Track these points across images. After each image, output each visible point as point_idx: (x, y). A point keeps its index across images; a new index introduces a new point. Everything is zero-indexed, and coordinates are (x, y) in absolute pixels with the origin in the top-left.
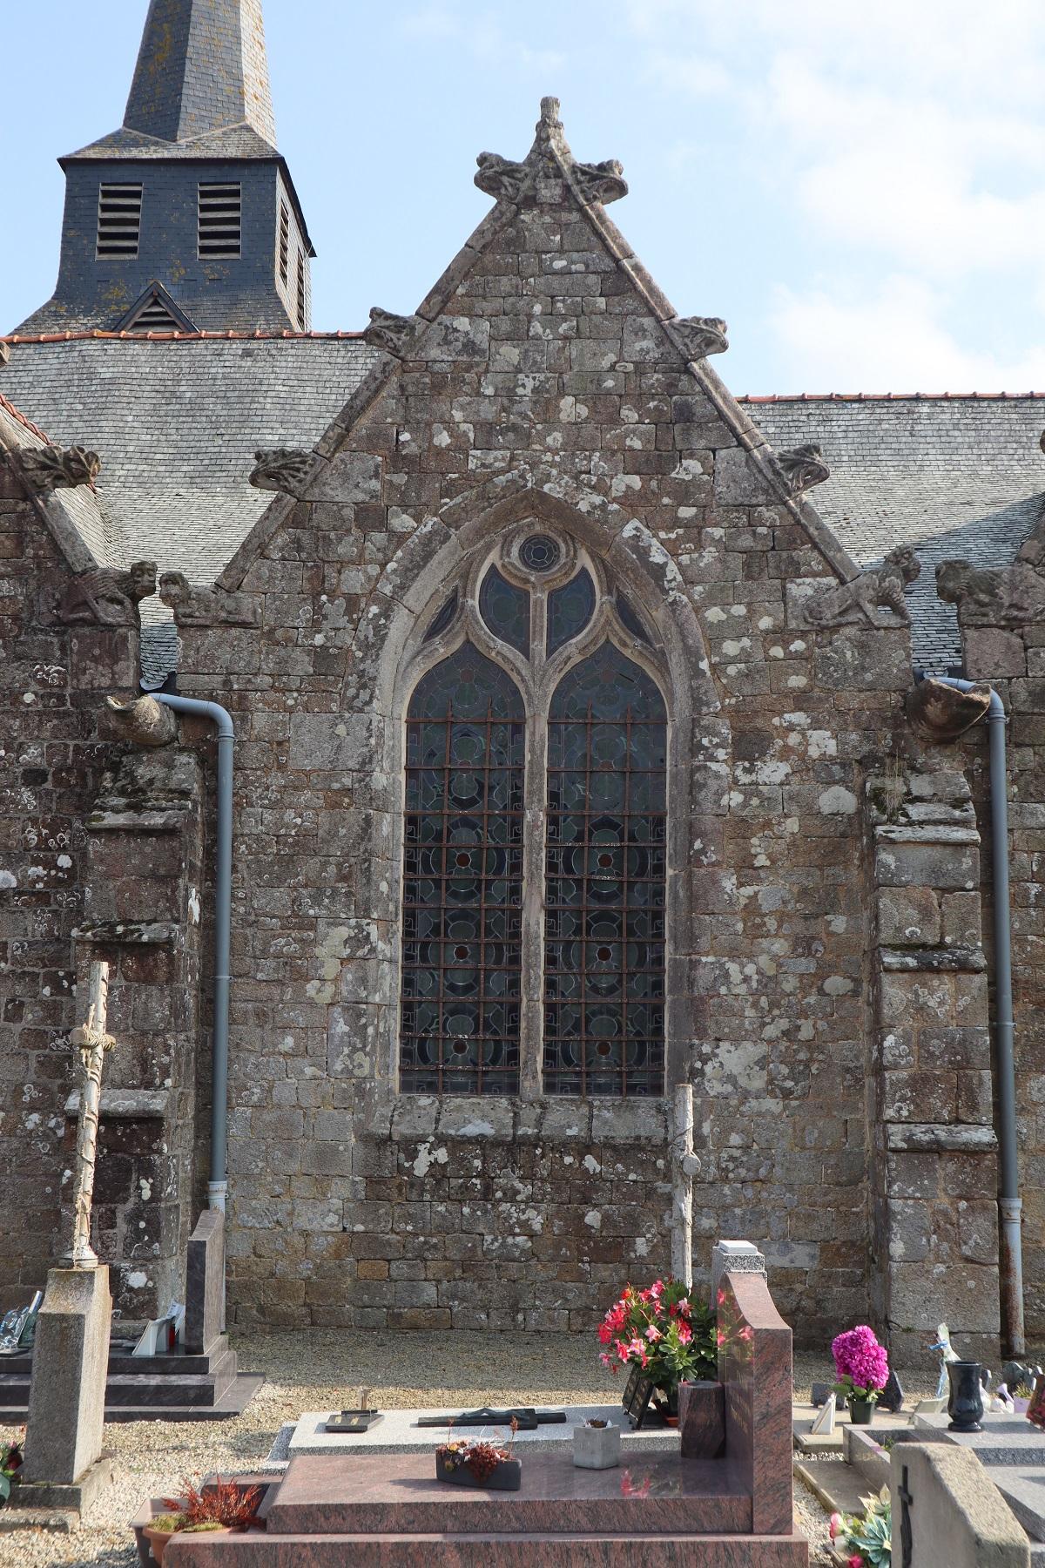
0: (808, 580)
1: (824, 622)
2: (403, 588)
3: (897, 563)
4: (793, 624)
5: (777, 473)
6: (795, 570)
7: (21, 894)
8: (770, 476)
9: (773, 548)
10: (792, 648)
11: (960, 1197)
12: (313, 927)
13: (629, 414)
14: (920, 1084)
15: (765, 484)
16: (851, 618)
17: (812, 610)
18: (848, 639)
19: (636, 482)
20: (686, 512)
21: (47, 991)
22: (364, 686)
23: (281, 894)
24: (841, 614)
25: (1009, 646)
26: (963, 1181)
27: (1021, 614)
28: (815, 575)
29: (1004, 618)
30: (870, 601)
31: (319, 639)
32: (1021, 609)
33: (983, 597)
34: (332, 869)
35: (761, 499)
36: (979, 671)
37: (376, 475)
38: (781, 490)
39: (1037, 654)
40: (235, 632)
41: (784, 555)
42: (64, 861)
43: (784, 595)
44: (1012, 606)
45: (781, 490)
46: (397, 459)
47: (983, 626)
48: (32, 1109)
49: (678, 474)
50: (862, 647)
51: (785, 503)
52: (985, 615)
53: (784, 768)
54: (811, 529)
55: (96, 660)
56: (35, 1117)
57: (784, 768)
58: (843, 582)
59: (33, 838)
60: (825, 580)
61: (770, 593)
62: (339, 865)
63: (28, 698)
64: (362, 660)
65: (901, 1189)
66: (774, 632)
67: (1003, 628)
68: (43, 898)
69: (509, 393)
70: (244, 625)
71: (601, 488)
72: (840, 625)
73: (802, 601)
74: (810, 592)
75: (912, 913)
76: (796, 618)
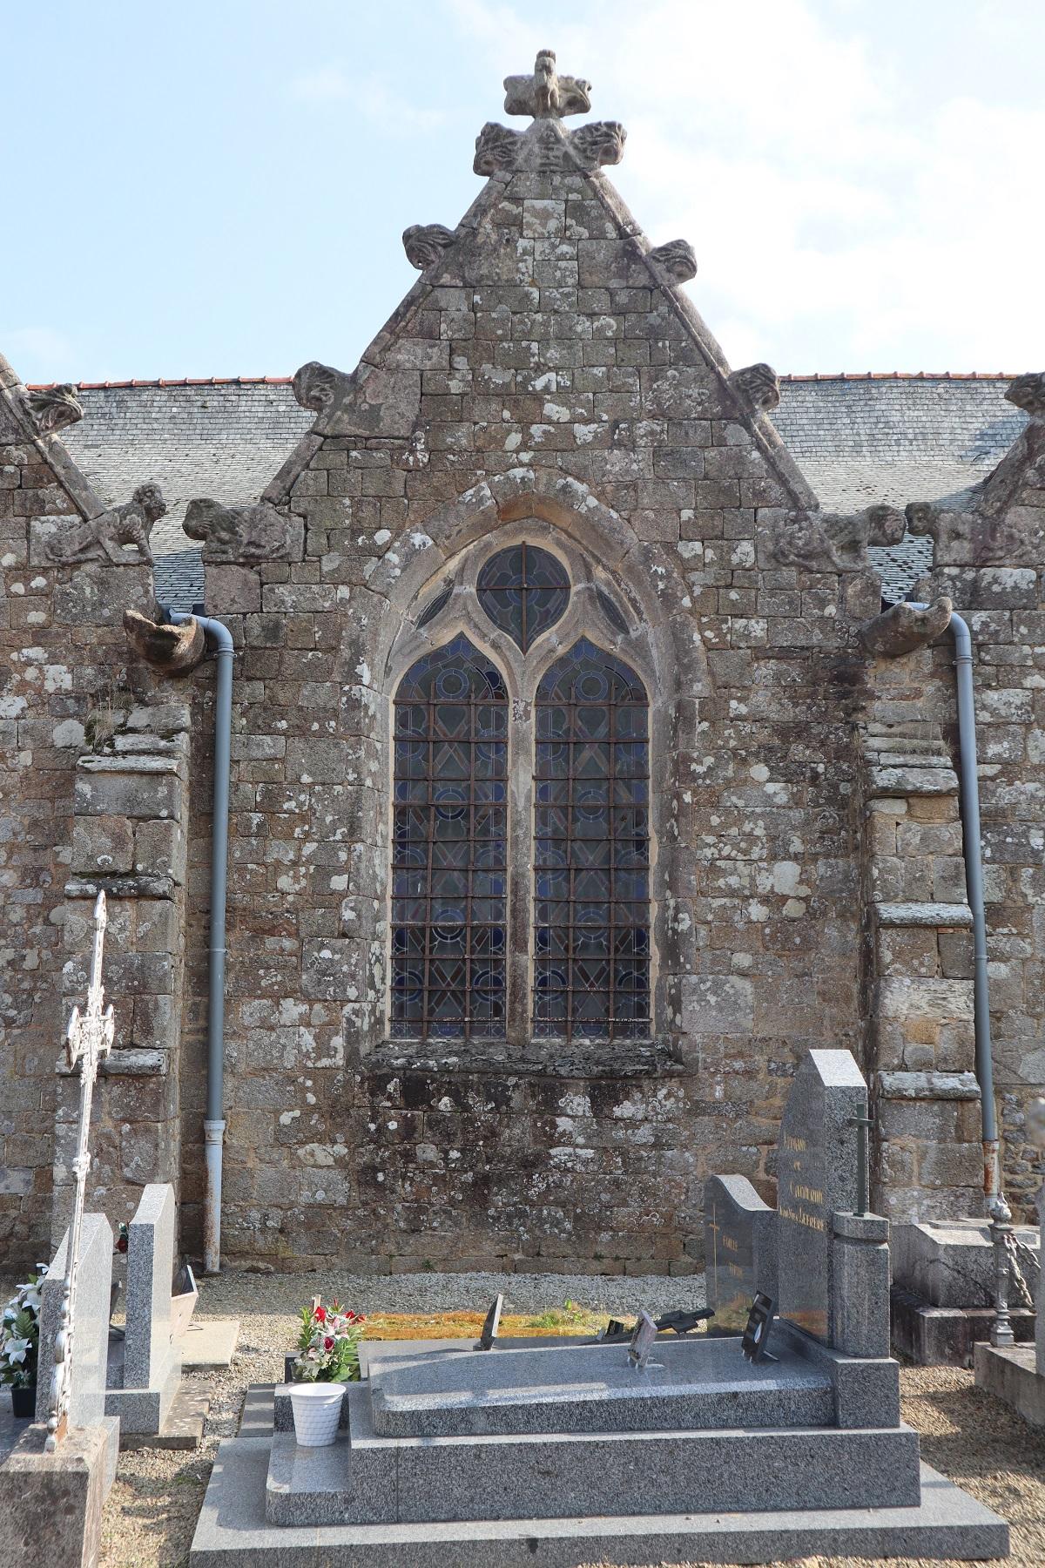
0: (52, 518)
1: (64, 559)
3: (140, 501)
4: (35, 561)
5: (27, 413)
6: (40, 508)
8: (20, 415)
9: (20, 487)
10: (33, 584)
11: (124, 1120)
15: (15, 423)
16: (90, 555)
17: (54, 548)
24: (81, 551)
25: (246, 582)
26: (128, 1105)
27: (257, 552)
28: (59, 513)
29: (242, 555)
30: (111, 539)
32: (259, 546)
33: (225, 535)
35: (11, 438)
36: (215, 607)
38: (29, 430)
39: (272, 590)
41: (30, 493)
43: (28, 532)
44: (250, 543)
45: (29, 430)
47: (223, 563)
50: (102, 583)
51: (33, 442)
52: (224, 552)
53: (21, 702)
54: (58, 469)
57: (21, 702)
58: (85, 520)
60: (69, 518)
61: (14, 530)
65: (66, 1114)
66: (17, 569)
67: (242, 565)
72: (80, 562)
73: (45, 538)
74: (54, 529)
75: (106, 841)
76: (38, 555)
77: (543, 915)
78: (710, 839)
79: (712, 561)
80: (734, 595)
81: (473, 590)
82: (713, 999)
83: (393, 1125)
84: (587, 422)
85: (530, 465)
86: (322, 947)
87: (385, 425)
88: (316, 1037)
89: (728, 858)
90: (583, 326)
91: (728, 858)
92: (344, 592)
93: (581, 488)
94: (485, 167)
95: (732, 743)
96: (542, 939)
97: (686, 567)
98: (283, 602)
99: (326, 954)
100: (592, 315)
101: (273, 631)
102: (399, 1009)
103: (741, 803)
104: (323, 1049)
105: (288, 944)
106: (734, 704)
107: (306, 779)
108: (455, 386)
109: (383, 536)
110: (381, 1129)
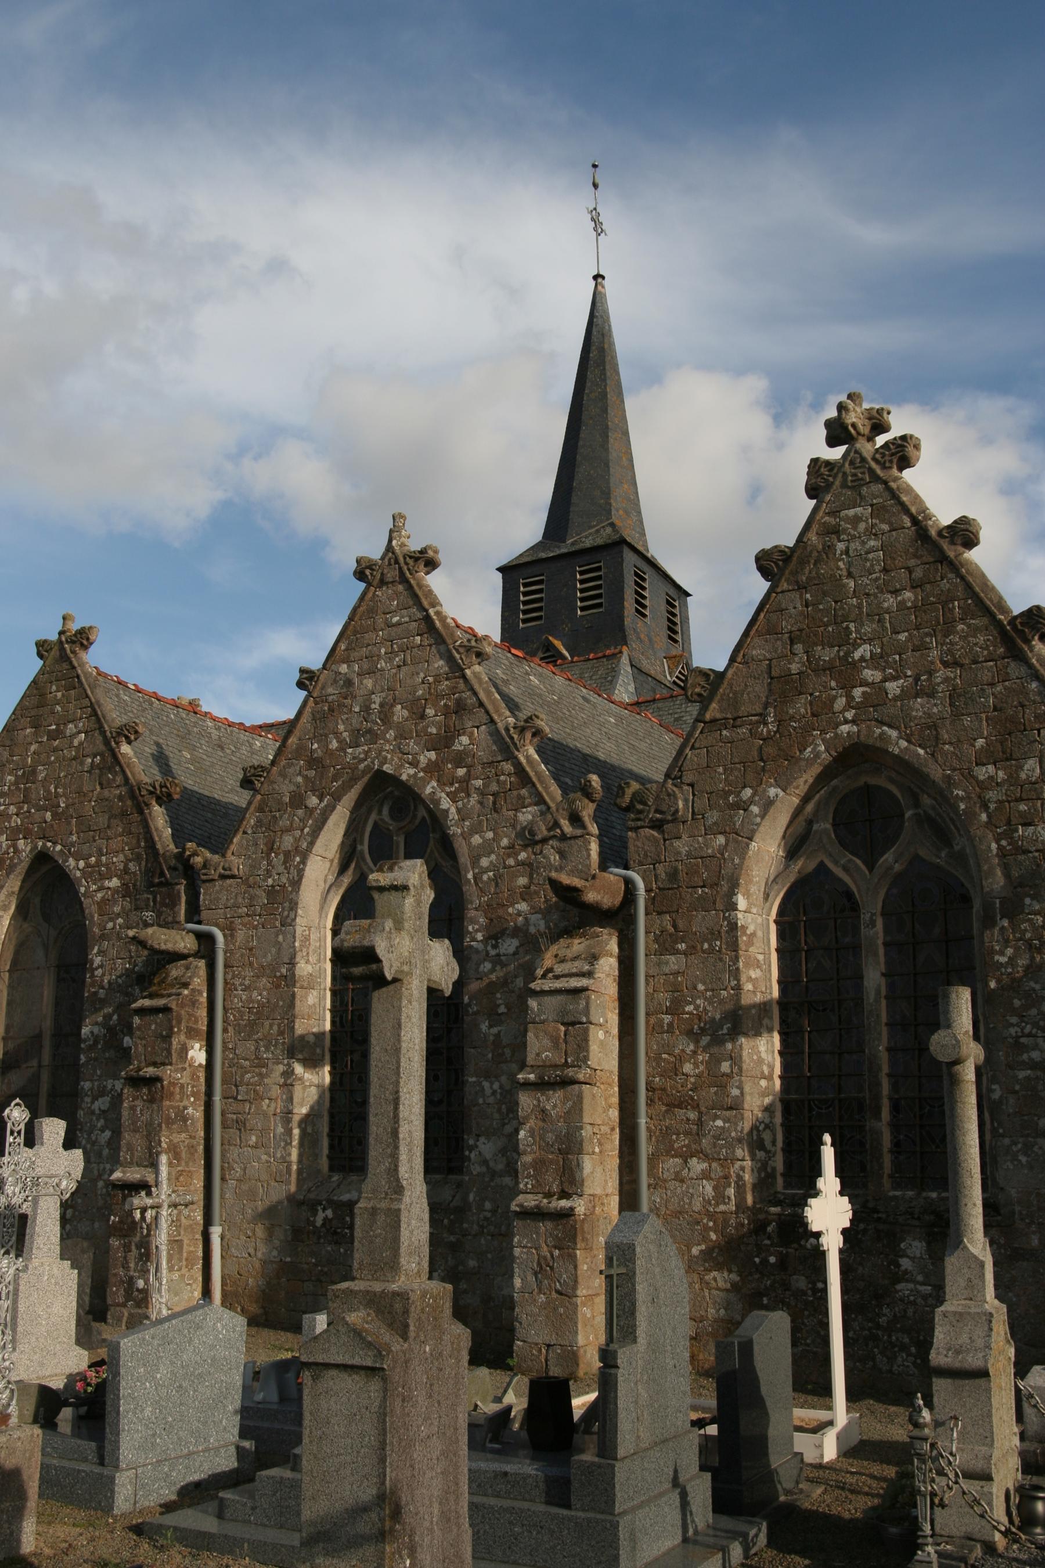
2: (312, 844)
10: (519, 858)
11: (555, 1248)
12: (266, 1066)
13: (430, 712)
14: (539, 1165)
18: (553, 847)
19: (432, 755)
20: (461, 772)
22: (291, 909)
23: (251, 1045)
26: (557, 1236)
31: (270, 881)
34: (275, 1028)
37: (300, 774)
40: (229, 881)
46: (313, 762)
49: (457, 747)
50: (562, 854)
53: (515, 942)
57: (515, 942)
62: (279, 1025)
64: (291, 892)
65: (519, 1241)
69: (366, 709)
70: (233, 877)
71: (414, 764)
74: (530, 817)
75: (546, 1042)
77: (895, 1087)
78: (1014, 1020)
79: (1004, 780)
80: (1023, 807)
81: (828, 826)
82: (1024, 1159)
83: (772, 1260)
84: (895, 678)
85: (853, 722)
86: (716, 1117)
87: (743, 710)
88: (715, 1188)
89: (1030, 1035)
90: (890, 602)
91: (1030, 1035)
92: (721, 840)
93: (894, 734)
94: (813, 493)
95: (1028, 935)
96: (895, 1108)
97: (983, 786)
98: (679, 853)
99: (719, 1123)
100: (895, 592)
101: (673, 875)
102: (788, 1165)
103: (1037, 987)
104: (720, 1197)
105: (693, 1115)
106: (1028, 901)
107: (701, 987)
108: (795, 668)
109: (748, 792)
110: (765, 1262)
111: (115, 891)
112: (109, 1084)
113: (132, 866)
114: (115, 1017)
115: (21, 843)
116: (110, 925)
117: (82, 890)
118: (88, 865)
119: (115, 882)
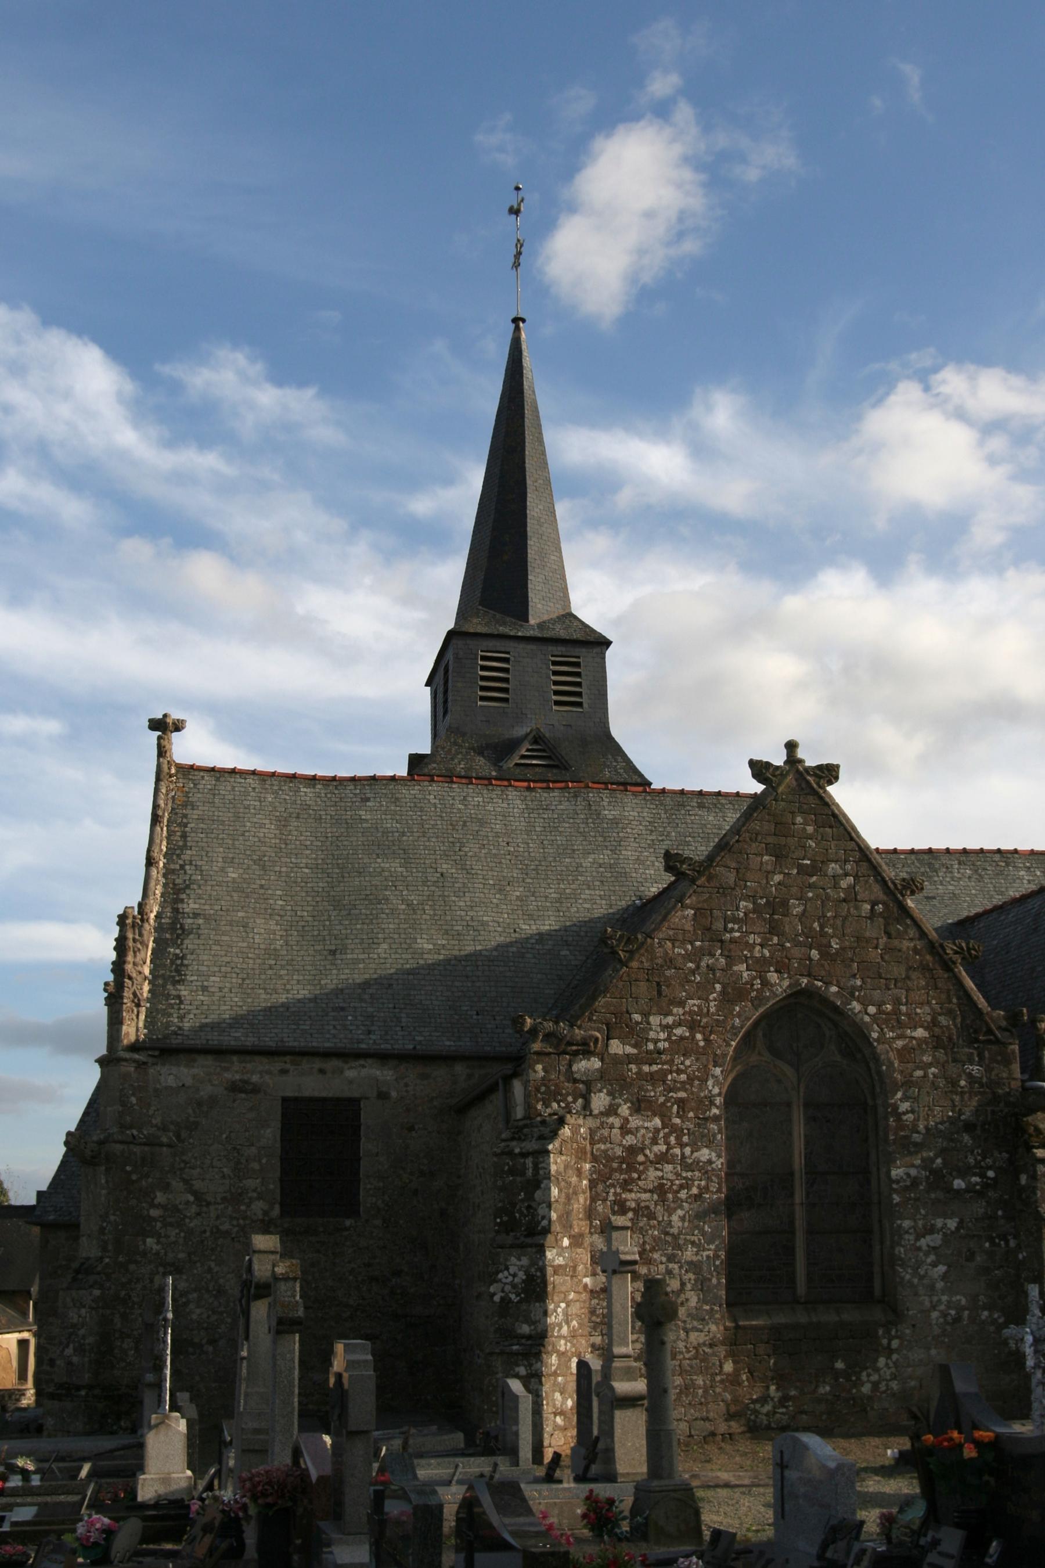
7: (969, 1192)
21: (987, 1245)
42: (991, 1174)
48: (984, 1308)
55: (998, 1062)
56: (986, 1313)
59: (972, 1161)
63: (963, 1083)
68: (980, 1194)
111: (921, 1041)
112: (939, 1223)
113: (943, 1020)
114: (939, 1161)
115: (773, 977)
116: (919, 1073)
117: (875, 1035)
118: (880, 1012)
119: (920, 1033)
